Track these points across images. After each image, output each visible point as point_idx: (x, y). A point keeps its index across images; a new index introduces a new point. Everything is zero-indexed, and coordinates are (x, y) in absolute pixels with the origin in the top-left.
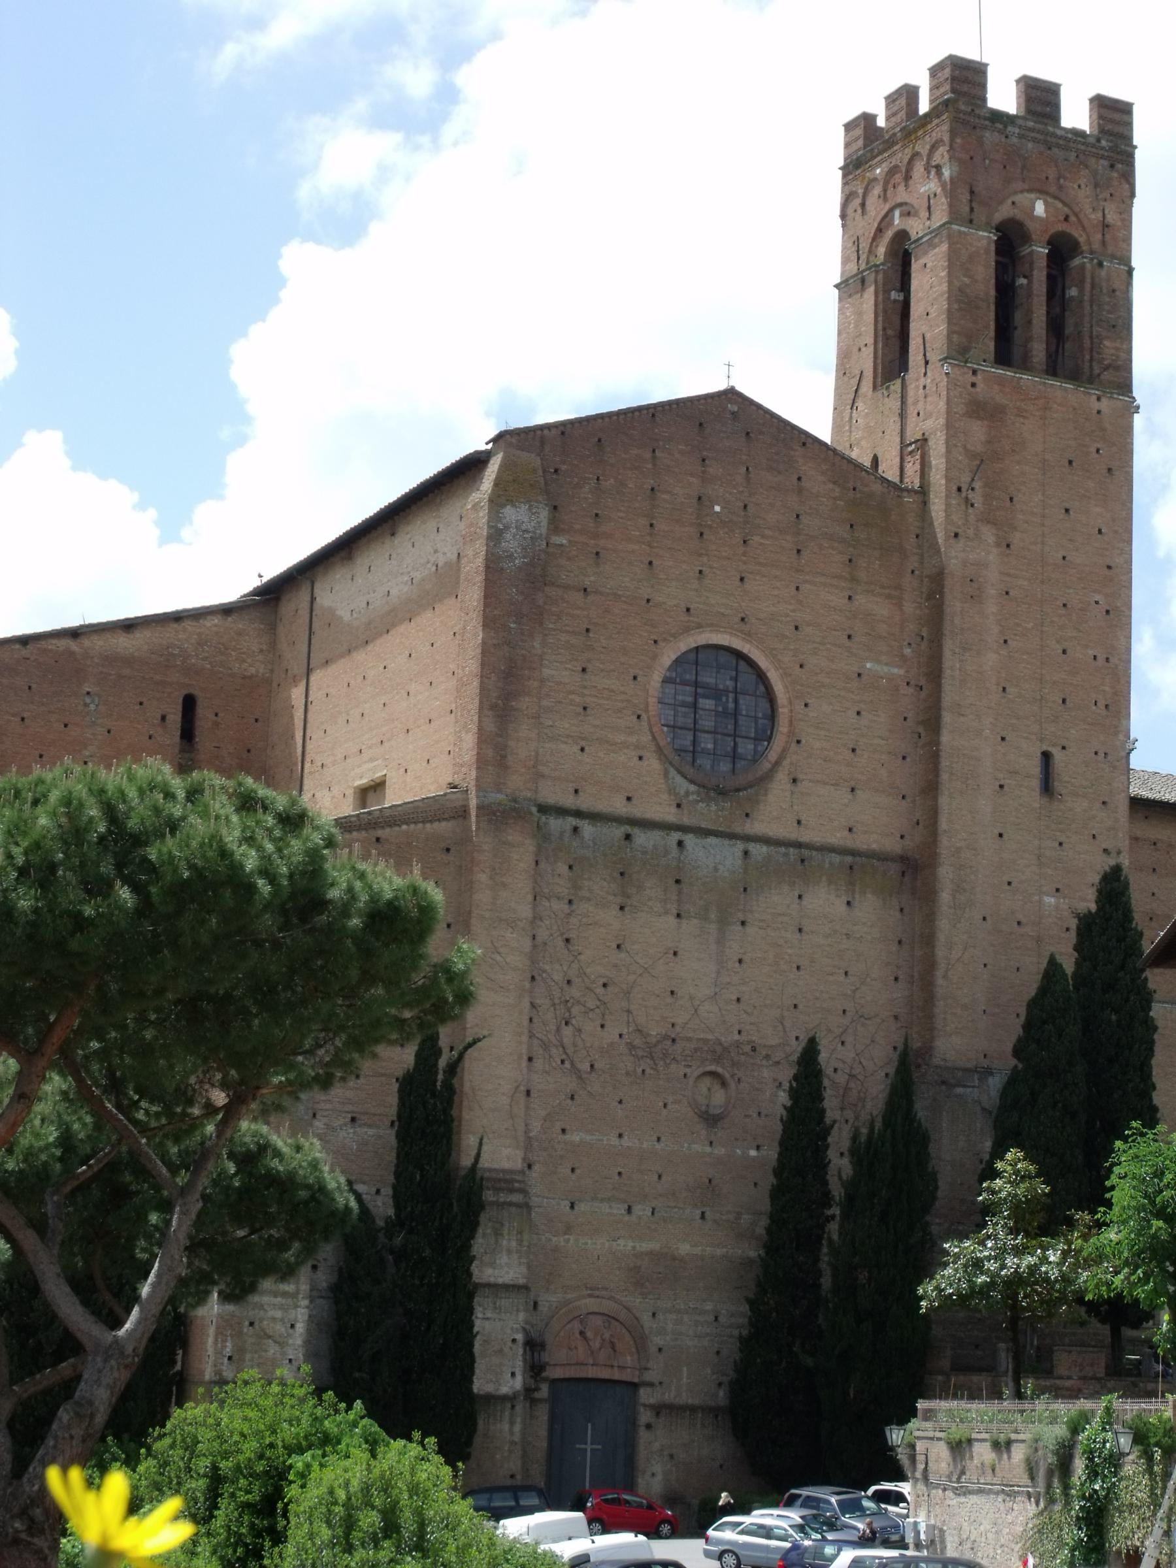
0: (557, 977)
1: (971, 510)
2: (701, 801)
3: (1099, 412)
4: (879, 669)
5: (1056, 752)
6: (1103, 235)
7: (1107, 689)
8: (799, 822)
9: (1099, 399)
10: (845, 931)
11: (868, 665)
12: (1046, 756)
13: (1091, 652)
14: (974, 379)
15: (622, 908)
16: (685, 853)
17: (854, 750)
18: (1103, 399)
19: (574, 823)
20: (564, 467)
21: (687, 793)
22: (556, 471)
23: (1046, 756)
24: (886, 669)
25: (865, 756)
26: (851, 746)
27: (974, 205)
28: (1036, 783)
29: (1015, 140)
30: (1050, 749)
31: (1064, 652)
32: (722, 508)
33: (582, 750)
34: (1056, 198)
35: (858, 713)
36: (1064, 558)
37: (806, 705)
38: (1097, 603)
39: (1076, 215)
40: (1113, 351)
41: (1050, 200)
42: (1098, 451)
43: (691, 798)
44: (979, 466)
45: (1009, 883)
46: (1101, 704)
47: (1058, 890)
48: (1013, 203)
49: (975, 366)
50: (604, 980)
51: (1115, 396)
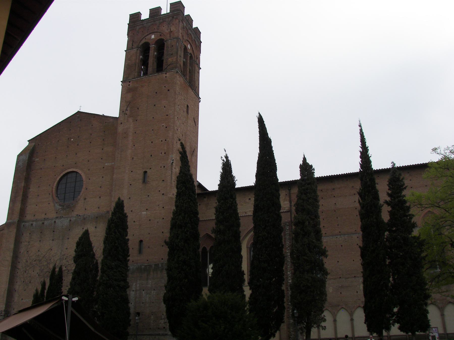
0: (24, 261)
1: (126, 116)
2: (62, 210)
3: (166, 77)
4: (109, 164)
5: (148, 171)
6: (170, 34)
7: (165, 148)
8: (86, 209)
9: (166, 74)
10: (94, 235)
11: (106, 164)
12: (145, 172)
13: (160, 140)
14: (129, 84)
15: (40, 241)
16: (56, 224)
17: (101, 187)
18: (167, 73)
19: (32, 223)
20: (40, 143)
21: (59, 209)
22: (38, 145)
23: (145, 172)
24: (111, 164)
25: (104, 188)
26: (100, 186)
27: (133, 44)
28: (141, 181)
29: (145, 25)
30: (146, 170)
31: (152, 142)
32: (73, 139)
33: (37, 205)
34: (157, 32)
35: (103, 177)
36: (153, 118)
37: (89, 179)
38: (163, 126)
39: (162, 34)
40: (171, 60)
42: (165, 87)
43: (60, 210)
44: (129, 104)
45: (132, 211)
46: (163, 153)
47: (147, 209)
48: (145, 39)
49: (129, 81)
50: (35, 260)
51: (170, 71)
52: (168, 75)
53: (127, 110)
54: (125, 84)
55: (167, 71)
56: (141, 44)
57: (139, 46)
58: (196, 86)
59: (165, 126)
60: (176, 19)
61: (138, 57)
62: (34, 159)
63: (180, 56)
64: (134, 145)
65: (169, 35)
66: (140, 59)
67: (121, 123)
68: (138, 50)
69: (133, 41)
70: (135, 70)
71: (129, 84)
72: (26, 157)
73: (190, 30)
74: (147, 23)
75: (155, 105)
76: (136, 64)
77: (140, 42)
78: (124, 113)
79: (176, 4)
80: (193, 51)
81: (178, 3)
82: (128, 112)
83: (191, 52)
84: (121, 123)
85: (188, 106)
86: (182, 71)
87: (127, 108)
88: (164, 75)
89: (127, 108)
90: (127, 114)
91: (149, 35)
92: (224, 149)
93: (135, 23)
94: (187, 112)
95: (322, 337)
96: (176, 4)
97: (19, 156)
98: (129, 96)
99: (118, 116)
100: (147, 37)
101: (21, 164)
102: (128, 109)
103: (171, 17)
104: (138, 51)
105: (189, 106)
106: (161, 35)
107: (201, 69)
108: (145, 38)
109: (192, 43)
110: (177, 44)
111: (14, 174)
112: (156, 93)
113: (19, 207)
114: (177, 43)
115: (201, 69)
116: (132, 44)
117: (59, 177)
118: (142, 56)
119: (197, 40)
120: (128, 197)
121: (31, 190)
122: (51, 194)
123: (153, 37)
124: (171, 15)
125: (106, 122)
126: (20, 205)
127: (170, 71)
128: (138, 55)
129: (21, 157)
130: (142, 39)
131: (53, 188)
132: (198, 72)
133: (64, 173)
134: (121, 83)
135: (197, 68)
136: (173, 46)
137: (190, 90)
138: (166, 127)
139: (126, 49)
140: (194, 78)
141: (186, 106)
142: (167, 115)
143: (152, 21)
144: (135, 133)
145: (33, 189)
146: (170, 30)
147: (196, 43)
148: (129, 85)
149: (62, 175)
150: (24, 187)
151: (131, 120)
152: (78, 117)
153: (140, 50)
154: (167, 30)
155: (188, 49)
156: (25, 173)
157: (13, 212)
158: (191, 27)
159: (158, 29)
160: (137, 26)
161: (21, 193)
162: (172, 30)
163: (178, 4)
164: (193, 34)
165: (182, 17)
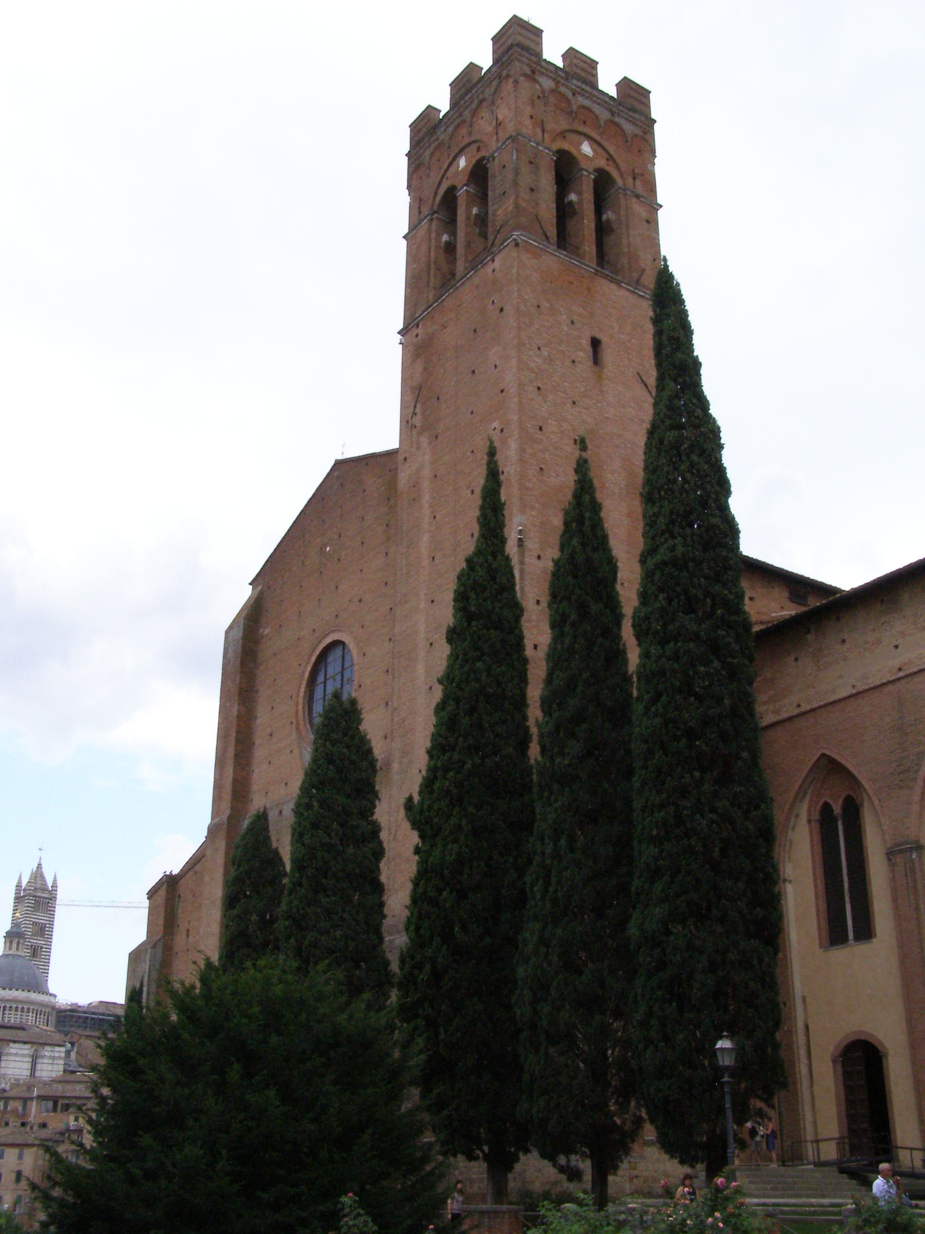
3: (494, 271)
9: (493, 260)
41: (466, 150)
48: (447, 178)
51: (502, 247)
52: (497, 264)
53: (416, 414)
54: (408, 336)
55: (492, 253)
56: (438, 198)
57: (435, 208)
58: (643, 266)
59: (499, 428)
60: (508, 76)
61: (433, 241)
62: (261, 630)
63: (532, 190)
64: (435, 517)
65: (495, 138)
66: (443, 245)
67: (405, 459)
68: (432, 220)
69: (421, 200)
70: (428, 283)
71: (417, 331)
72: (238, 633)
73: (583, 95)
74: (445, 130)
75: (473, 372)
76: (429, 266)
77: (436, 193)
78: (410, 423)
79: (507, 31)
80: (610, 158)
81: (508, 25)
82: (417, 421)
83: (602, 163)
84: (405, 459)
85: (595, 343)
86: (547, 238)
87: (415, 407)
88: (489, 268)
89: (415, 407)
90: (415, 427)
91: (455, 163)
92: (582, 444)
93: (421, 145)
94: (596, 359)
95: (917, 1143)
96: (504, 34)
97: (227, 632)
98: (419, 367)
99: (395, 445)
100: (449, 174)
101: (230, 651)
102: (418, 410)
103: (494, 79)
104: (434, 223)
105: (605, 339)
106: (479, 149)
107: (661, 206)
108: (446, 176)
109: (601, 134)
110: (512, 155)
111: (220, 684)
112: (475, 330)
113: (231, 776)
114: (515, 152)
115: (661, 206)
116: (419, 208)
117: (309, 668)
118: (446, 233)
119: (626, 119)
120: (428, 687)
121: (259, 721)
122: (295, 723)
123: (462, 162)
124: (496, 72)
125: (390, 471)
126: (231, 771)
127: (502, 247)
128: (434, 235)
129: (231, 634)
130: (440, 182)
131: (297, 703)
132: (648, 222)
133: (317, 652)
134: (399, 337)
135: (638, 208)
136: (504, 167)
137: (606, 288)
138: (502, 431)
139: (406, 231)
140: (629, 245)
141: (586, 343)
142: (502, 391)
143: (454, 117)
144: (436, 476)
145: (262, 718)
146: (497, 119)
147: (623, 130)
148: (417, 336)
149: (313, 659)
150: (239, 717)
151: (424, 441)
152: (338, 478)
153: (437, 217)
154: (490, 123)
155: (579, 158)
156: (238, 676)
157: (220, 792)
158: (584, 86)
159: (470, 133)
160: (425, 150)
161: (234, 735)
162: (500, 117)
163: (510, 28)
164: (599, 104)
165: (528, 65)
